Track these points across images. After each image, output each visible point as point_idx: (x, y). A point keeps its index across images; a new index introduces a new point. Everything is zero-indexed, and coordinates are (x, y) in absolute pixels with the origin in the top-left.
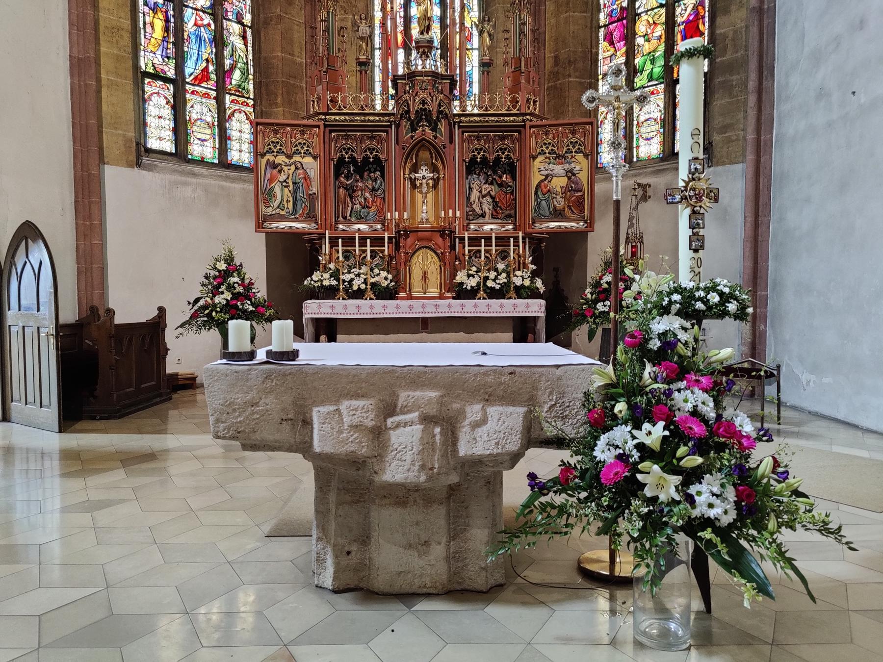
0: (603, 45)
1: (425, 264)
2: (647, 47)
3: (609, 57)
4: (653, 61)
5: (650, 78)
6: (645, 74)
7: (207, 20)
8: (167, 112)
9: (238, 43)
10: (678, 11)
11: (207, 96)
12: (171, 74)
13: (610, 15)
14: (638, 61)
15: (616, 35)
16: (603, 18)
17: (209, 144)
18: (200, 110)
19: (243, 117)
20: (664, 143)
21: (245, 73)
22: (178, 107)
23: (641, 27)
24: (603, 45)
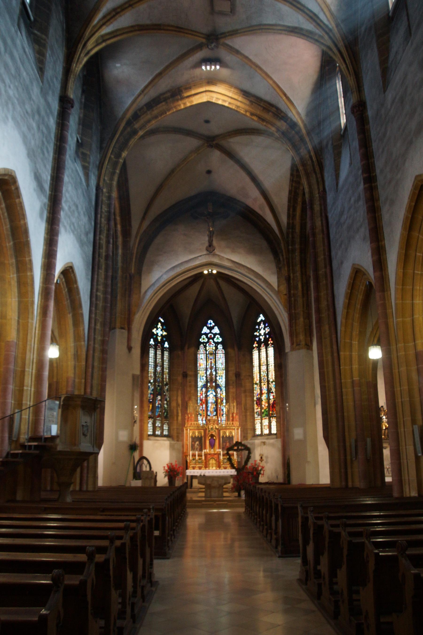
0: (255, 405)
1: (212, 462)
2: (265, 408)
3: (257, 409)
4: (266, 411)
5: (266, 415)
6: (265, 414)
7: (160, 402)
8: (151, 425)
9: (166, 406)
10: (270, 401)
11: (159, 420)
12: (153, 416)
13: (257, 398)
14: (263, 411)
15: (258, 403)
16: (255, 398)
17: (159, 431)
18: (158, 424)
19: (166, 424)
20: (269, 431)
21: (167, 412)
22: (154, 424)
23: (263, 403)
24: (255, 405)
